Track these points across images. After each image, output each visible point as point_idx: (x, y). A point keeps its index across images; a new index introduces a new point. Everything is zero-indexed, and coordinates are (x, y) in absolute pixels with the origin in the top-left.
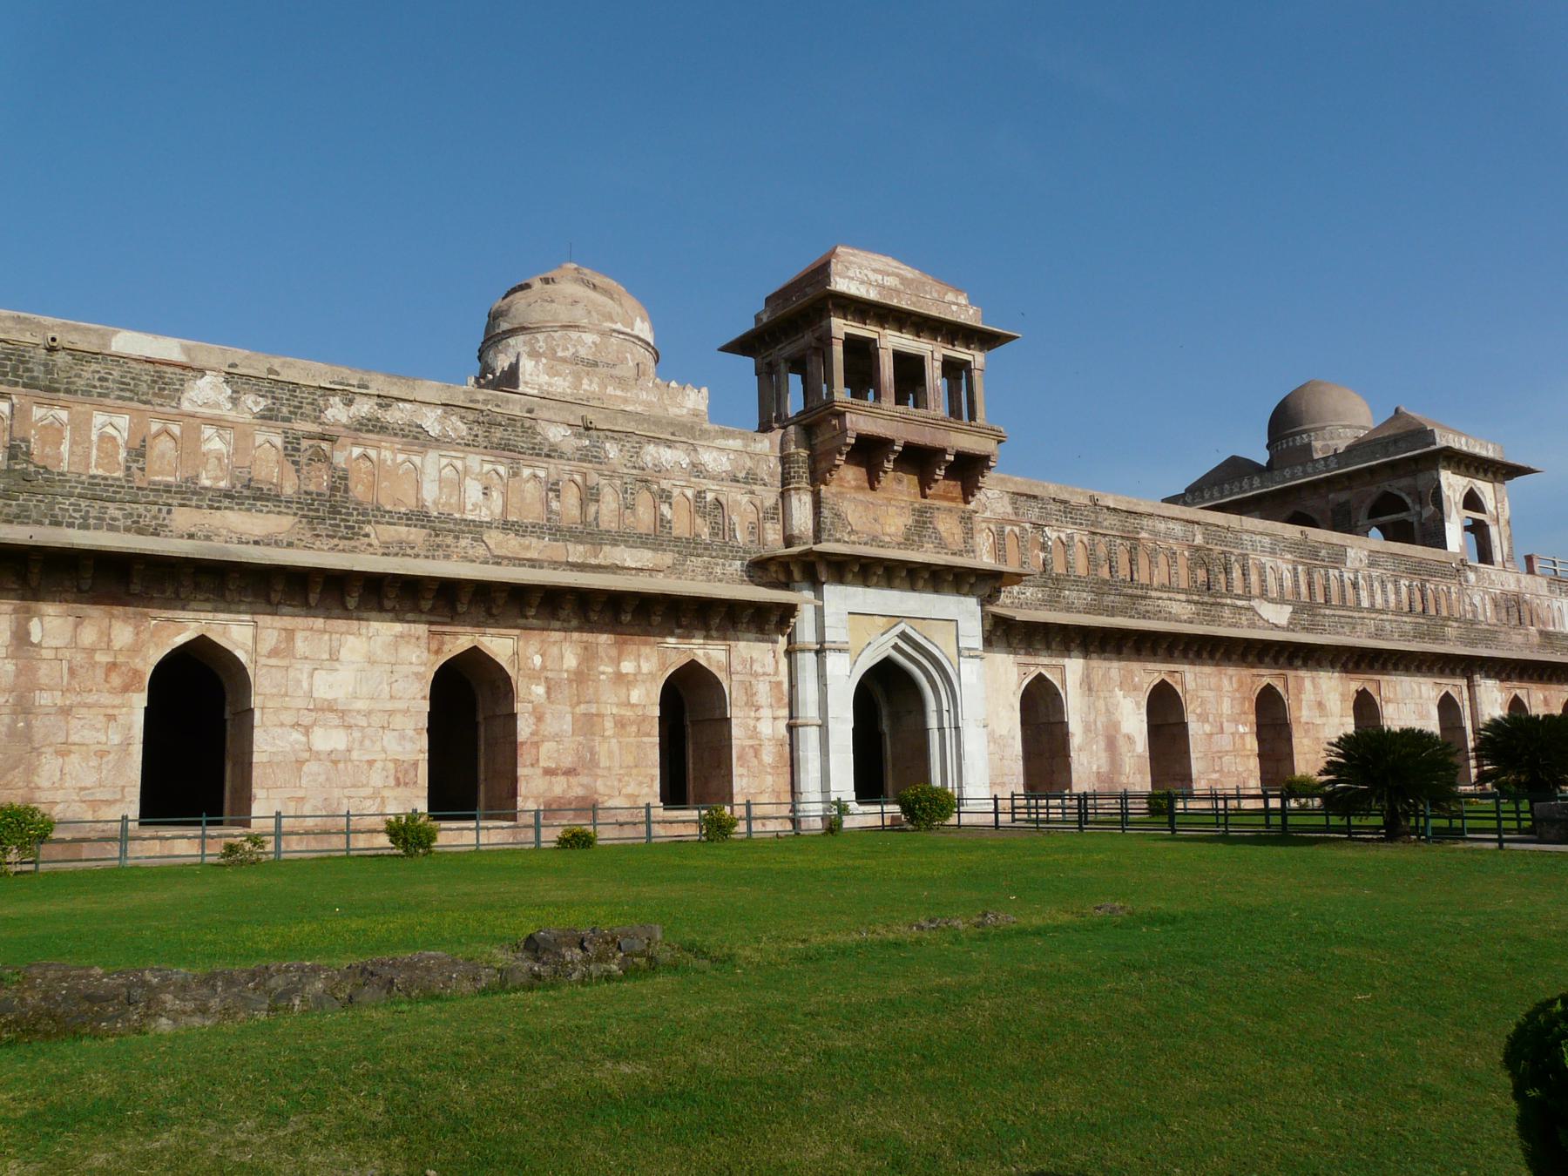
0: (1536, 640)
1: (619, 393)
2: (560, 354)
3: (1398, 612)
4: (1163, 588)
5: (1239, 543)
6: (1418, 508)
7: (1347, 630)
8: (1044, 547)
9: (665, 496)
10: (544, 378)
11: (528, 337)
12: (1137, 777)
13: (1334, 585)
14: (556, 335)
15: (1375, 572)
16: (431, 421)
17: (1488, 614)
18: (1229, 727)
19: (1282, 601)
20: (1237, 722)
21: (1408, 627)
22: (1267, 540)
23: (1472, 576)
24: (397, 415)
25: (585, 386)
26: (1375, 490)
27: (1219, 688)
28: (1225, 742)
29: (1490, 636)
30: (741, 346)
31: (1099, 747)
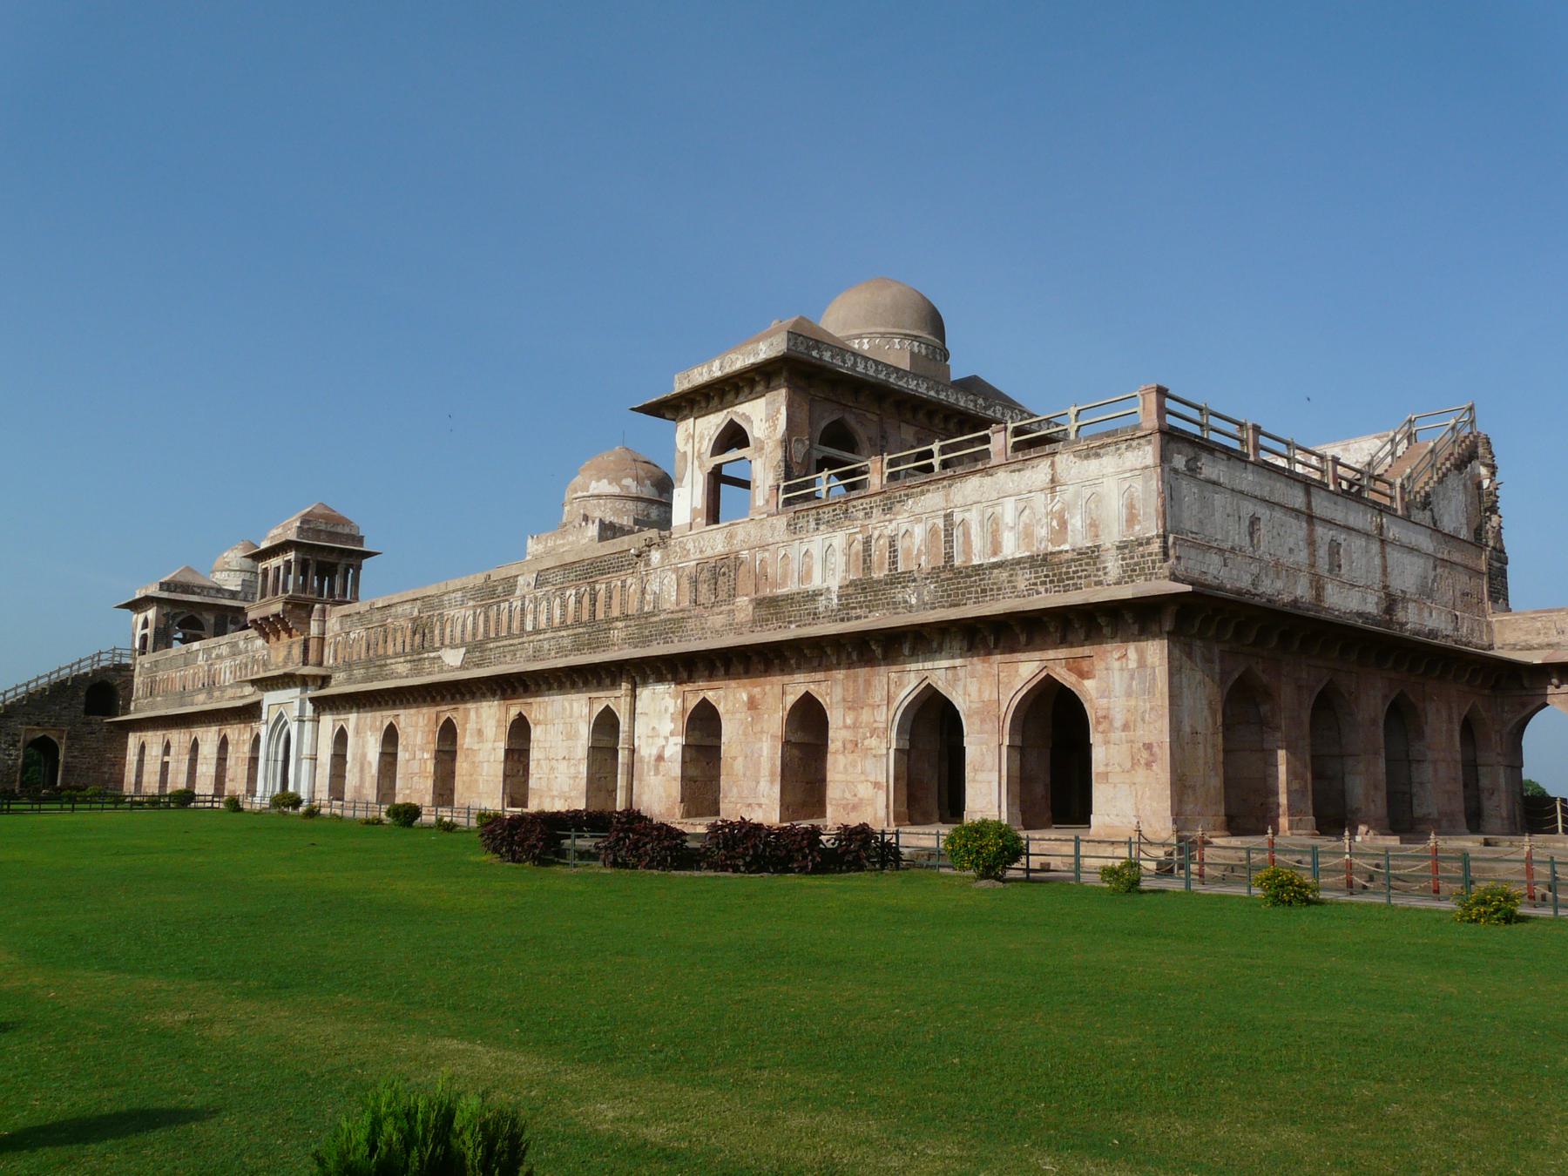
3: (564, 625)
4: (397, 655)
5: (441, 606)
7: (508, 658)
12: (371, 794)
13: (505, 617)
18: (419, 755)
20: (423, 750)
21: (567, 642)
22: (460, 594)
27: (416, 726)
28: (415, 766)
29: (676, 624)
31: (356, 770)
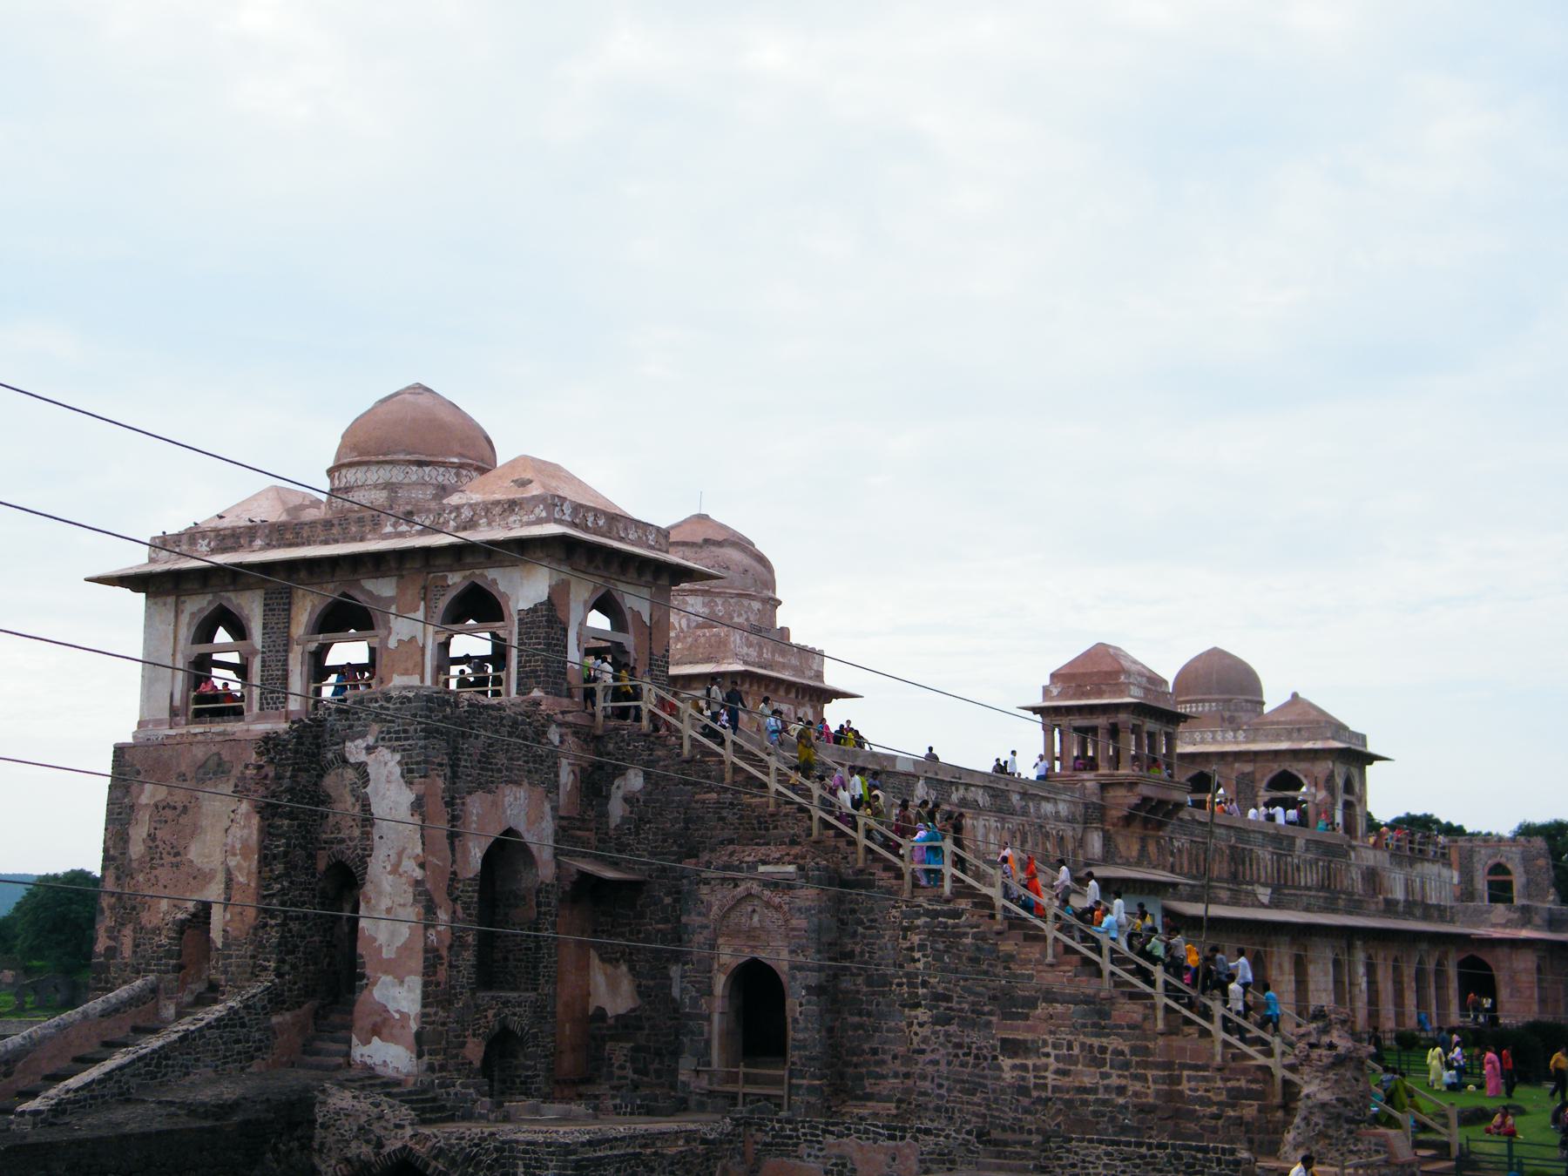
0: (1382, 906)
2: (736, 620)
4: (1220, 879)
8: (1172, 854)
9: (1047, 835)
11: (707, 599)
15: (1309, 856)
16: (982, 798)
17: (1359, 887)
19: (1265, 885)
23: (1353, 854)
24: (970, 796)
26: (1276, 768)
30: (1035, 710)
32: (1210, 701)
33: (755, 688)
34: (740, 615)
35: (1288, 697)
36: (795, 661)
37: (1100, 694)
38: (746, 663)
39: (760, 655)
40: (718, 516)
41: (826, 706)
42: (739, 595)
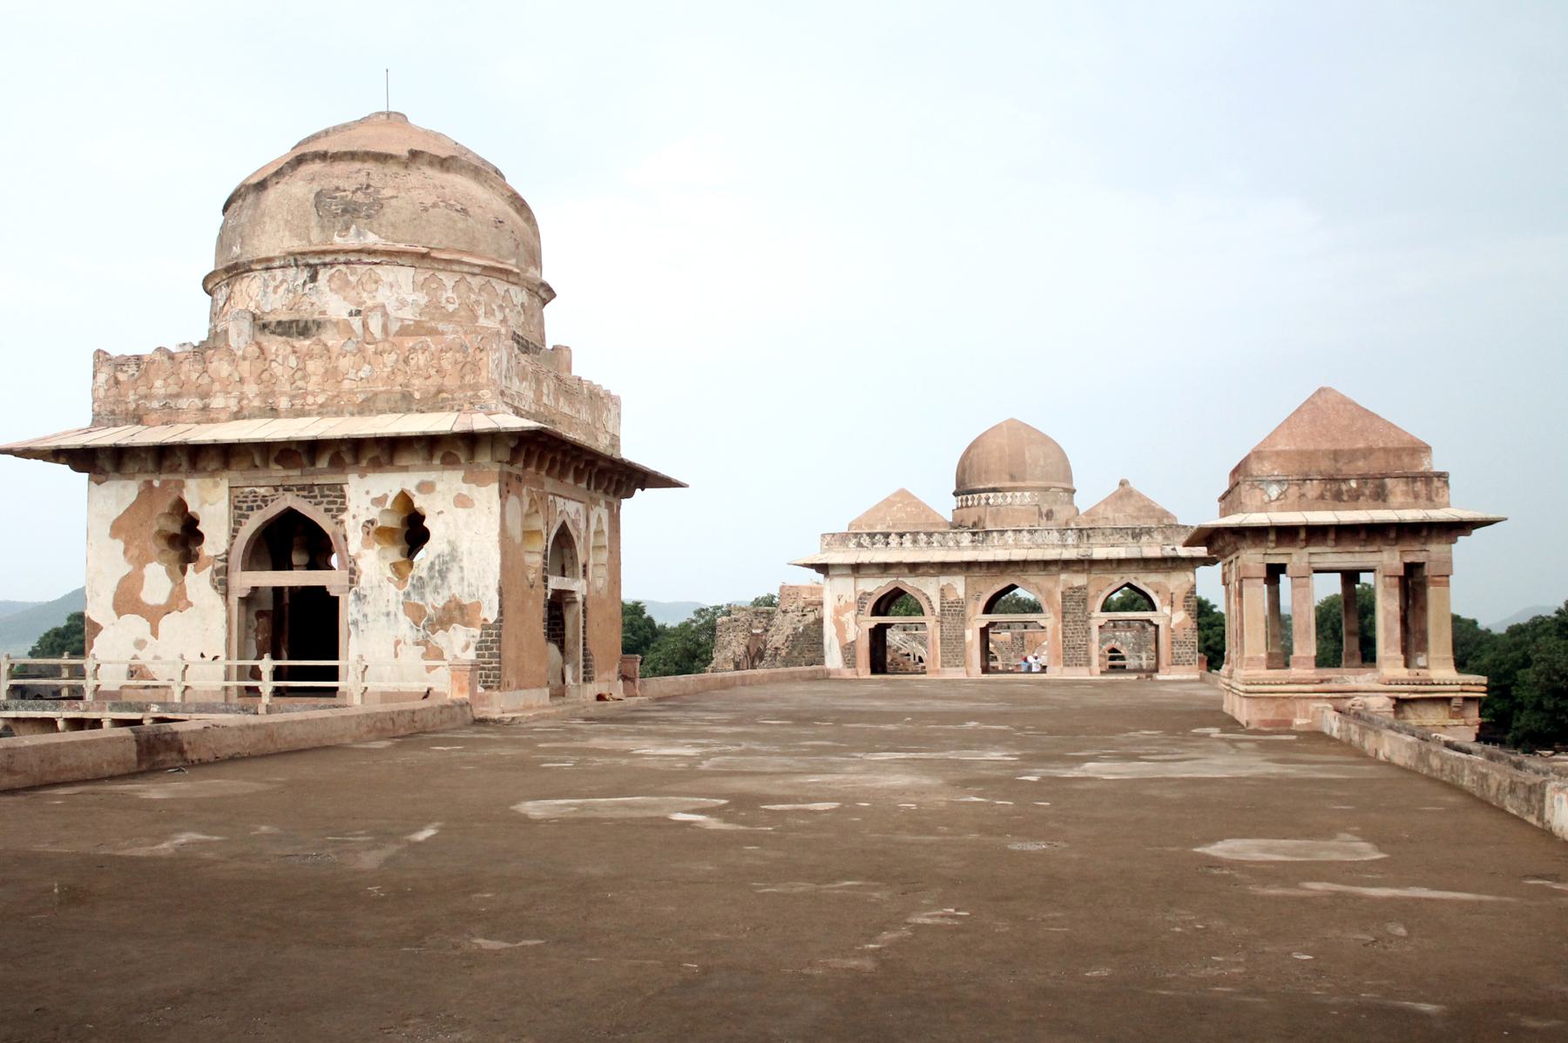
1: (566, 410)
6: (1167, 610)
10: (516, 381)
14: (476, 282)
25: (545, 400)
32: (1022, 489)
33: (532, 469)
34: (489, 313)
35: (1116, 487)
36: (585, 416)
37: (1380, 496)
38: (518, 412)
39: (538, 400)
40: (420, 118)
41: (624, 501)
42: (488, 270)
